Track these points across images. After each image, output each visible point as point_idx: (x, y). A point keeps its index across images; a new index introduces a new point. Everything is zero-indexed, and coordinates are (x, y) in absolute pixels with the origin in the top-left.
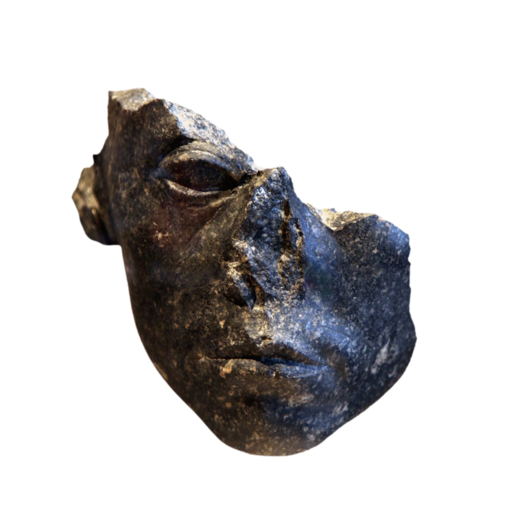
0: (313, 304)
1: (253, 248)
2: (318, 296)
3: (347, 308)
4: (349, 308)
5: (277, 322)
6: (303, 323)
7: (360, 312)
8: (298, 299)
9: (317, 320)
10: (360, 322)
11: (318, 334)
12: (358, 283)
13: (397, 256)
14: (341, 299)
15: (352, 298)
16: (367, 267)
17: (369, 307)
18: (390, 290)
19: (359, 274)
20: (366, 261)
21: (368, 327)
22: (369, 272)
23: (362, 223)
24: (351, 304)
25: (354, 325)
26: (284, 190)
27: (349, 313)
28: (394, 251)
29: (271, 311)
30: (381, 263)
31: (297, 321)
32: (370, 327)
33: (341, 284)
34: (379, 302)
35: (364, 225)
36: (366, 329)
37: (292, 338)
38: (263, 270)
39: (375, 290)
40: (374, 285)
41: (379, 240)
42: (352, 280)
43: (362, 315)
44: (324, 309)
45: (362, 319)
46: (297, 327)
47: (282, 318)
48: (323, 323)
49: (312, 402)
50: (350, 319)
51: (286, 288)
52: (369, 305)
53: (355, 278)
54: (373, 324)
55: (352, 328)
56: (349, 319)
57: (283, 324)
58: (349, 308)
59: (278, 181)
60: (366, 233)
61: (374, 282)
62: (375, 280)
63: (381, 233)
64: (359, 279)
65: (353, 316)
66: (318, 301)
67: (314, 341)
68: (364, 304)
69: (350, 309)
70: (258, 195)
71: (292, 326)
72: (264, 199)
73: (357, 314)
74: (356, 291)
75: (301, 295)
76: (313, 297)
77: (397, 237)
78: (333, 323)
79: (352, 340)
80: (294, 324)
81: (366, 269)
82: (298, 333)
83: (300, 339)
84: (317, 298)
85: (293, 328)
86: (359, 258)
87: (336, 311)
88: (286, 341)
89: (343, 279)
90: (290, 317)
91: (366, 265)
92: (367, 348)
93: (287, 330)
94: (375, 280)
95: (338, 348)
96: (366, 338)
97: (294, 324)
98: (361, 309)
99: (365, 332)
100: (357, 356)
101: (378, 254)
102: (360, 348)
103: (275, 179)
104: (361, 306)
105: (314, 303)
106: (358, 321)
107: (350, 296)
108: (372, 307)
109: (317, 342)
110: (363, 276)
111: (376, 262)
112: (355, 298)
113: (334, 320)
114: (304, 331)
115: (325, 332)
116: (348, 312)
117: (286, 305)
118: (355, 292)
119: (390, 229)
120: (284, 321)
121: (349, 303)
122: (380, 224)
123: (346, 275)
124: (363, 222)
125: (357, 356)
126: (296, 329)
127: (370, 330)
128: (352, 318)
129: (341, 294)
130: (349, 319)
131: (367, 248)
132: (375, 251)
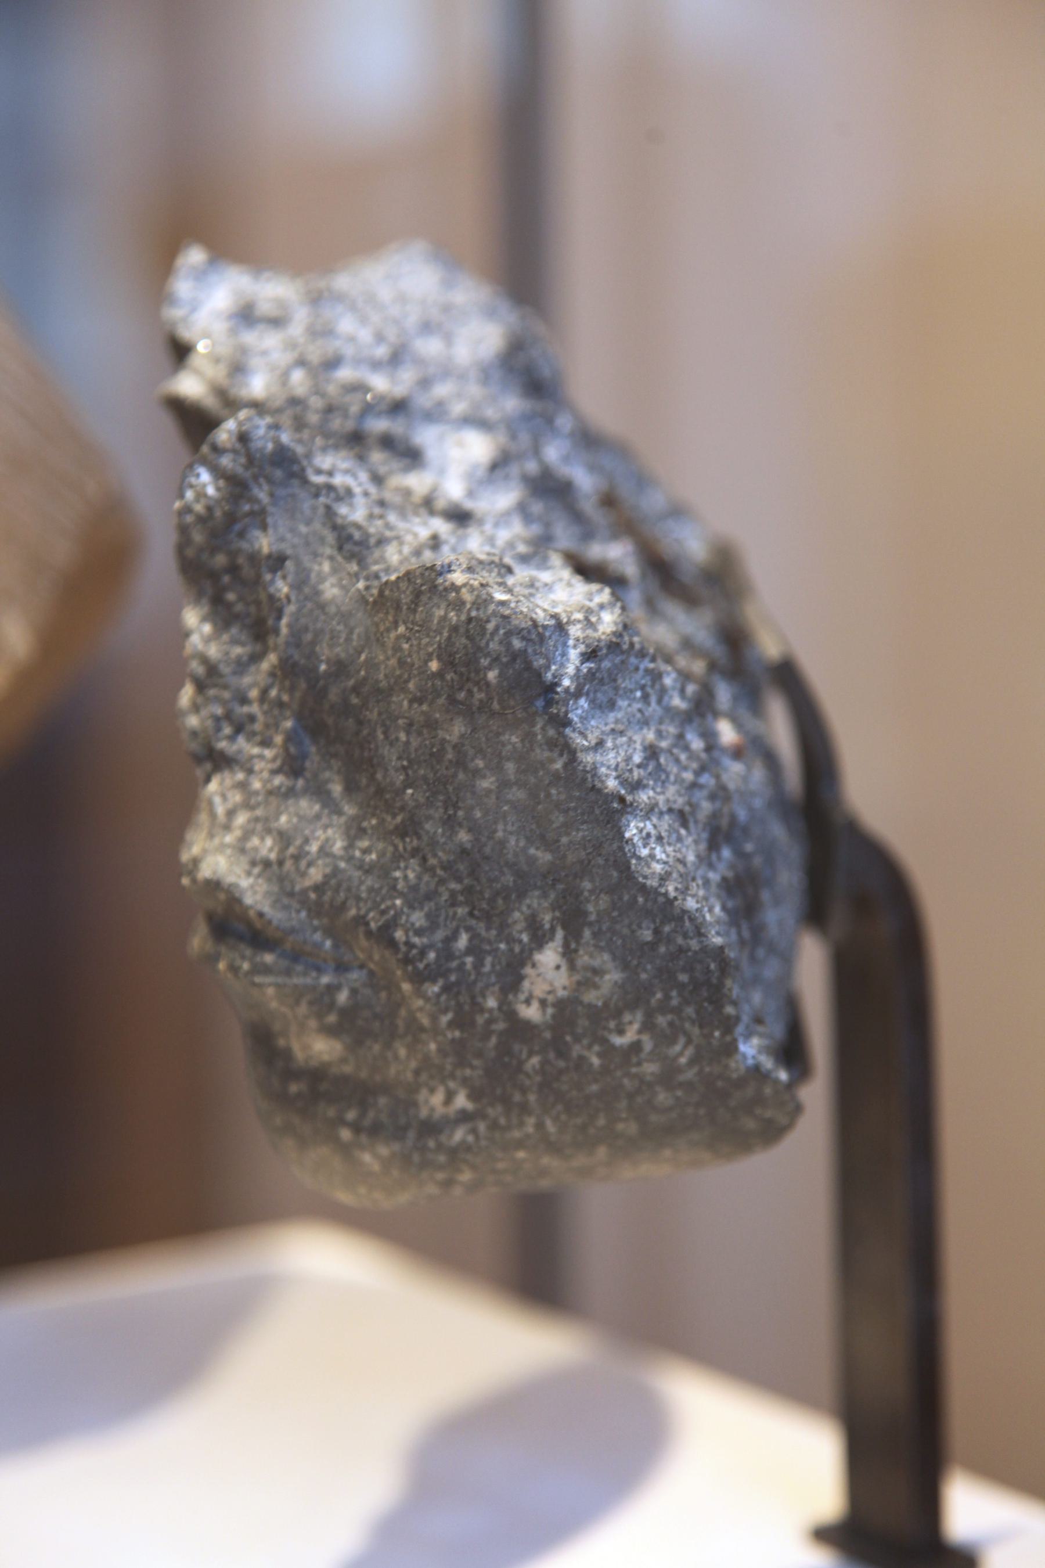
0: (320, 792)
1: (207, 628)
2: (339, 772)
3: (394, 816)
4: (399, 819)
5: (227, 828)
6: (284, 838)
7: (428, 832)
8: (286, 775)
9: (323, 837)
10: (432, 861)
11: (315, 875)
12: (412, 749)
13: (488, 684)
14: (380, 791)
15: (404, 792)
16: (425, 707)
17: (450, 823)
18: (504, 784)
19: (409, 727)
20: (421, 691)
21: (459, 879)
22: (431, 725)
23: (406, 583)
24: (402, 809)
25: (417, 868)
26: (256, 478)
27: (402, 832)
28: (477, 671)
29: (224, 797)
30: (452, 700)
31: (268, 831)
32: (466, 881)
33: (377, 748)
34: (478, 814)
35: (411, 588)
36: (453, 885)
37: (249, 874)
38: (215, 686)
39: (455, 776)
40: (450, 761)
41: (441, 634)
42: (397, 739)
43: (433, 843)
44: (350, 810)
45: (435, 855)
46: (266, 847)
47: (241, 819)
48: (338, 845)
49: (343, 1060)
50: (405, 849)
51: (266, 743)
52: (450, 816)
53: (403, 736)
54: (473, 873)
55: (411, 875)
56: (401, 848)
57: (238, 833)
58: (399, 819)
59: (234, 451)
60: (415, 611)
61: (450, 755)
62: (450, 749)
63: (446, 614)
64: (412, 740)
65: (412, 842)
66: (337, 789)
67: (304, 892)
68: (438, 813)
69: (403, 821)
70: (191, 486)
71: (255, 841)
72: (205, 495)
73: (419, 838)
74: (410, 772)
75: (292, 765)
76: (327, 774)
77: (484, 629)
78: (366, 851)
79: (412, 907)
80: (262, 839)
81: (422, 712)
82: (267, 864)
83: (269, 880)
84: (336, 778)
85: (256, 849)
86: (407, 681)
87: (374, 822)
88: (230, 879)
89: (381, 737)
90: (257, 820)
91: (420, 701)
92: (470, 940)
93: (242, 851)
94: (450, 749)
95: (367, 924)
96: (461, 911)
97: (262, 839)
98: (428, 826)
99: (453, 894)
100: (432, 955)
101: (440, 674)
102: (440, 935)
103: (228, 446)
104: (429, 818)
105: (328, 793)
106: (424, 859)
107: (398, 783)
108: (460, 825)
109: (313, 896)
110: (420, 734)
111: (439, 696)
112: (410, 791)
113: (365, 843)
114: (281, 863)
115: (336, 871)
116: (397, 828)
117: (257, 785)
118: (407, 775)
119: (468, 606)
120: (242, 827)
121: (398, 804)
122: (446, 589)
123: (384, 725)
124: (409, 580)
125: (432, 955)
126: (264, 852)
127: (468, 891)
128: (409, 848)
129: (379, 776)
130: (401, 848)
131: (418, 653)
132: (434, 665)
